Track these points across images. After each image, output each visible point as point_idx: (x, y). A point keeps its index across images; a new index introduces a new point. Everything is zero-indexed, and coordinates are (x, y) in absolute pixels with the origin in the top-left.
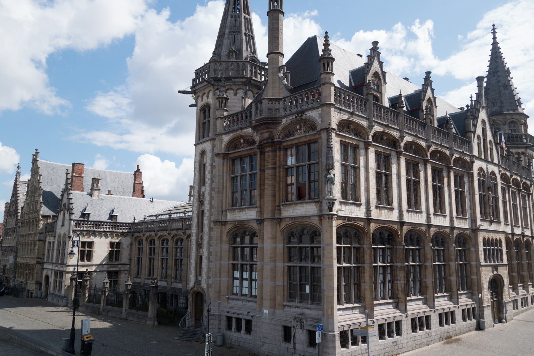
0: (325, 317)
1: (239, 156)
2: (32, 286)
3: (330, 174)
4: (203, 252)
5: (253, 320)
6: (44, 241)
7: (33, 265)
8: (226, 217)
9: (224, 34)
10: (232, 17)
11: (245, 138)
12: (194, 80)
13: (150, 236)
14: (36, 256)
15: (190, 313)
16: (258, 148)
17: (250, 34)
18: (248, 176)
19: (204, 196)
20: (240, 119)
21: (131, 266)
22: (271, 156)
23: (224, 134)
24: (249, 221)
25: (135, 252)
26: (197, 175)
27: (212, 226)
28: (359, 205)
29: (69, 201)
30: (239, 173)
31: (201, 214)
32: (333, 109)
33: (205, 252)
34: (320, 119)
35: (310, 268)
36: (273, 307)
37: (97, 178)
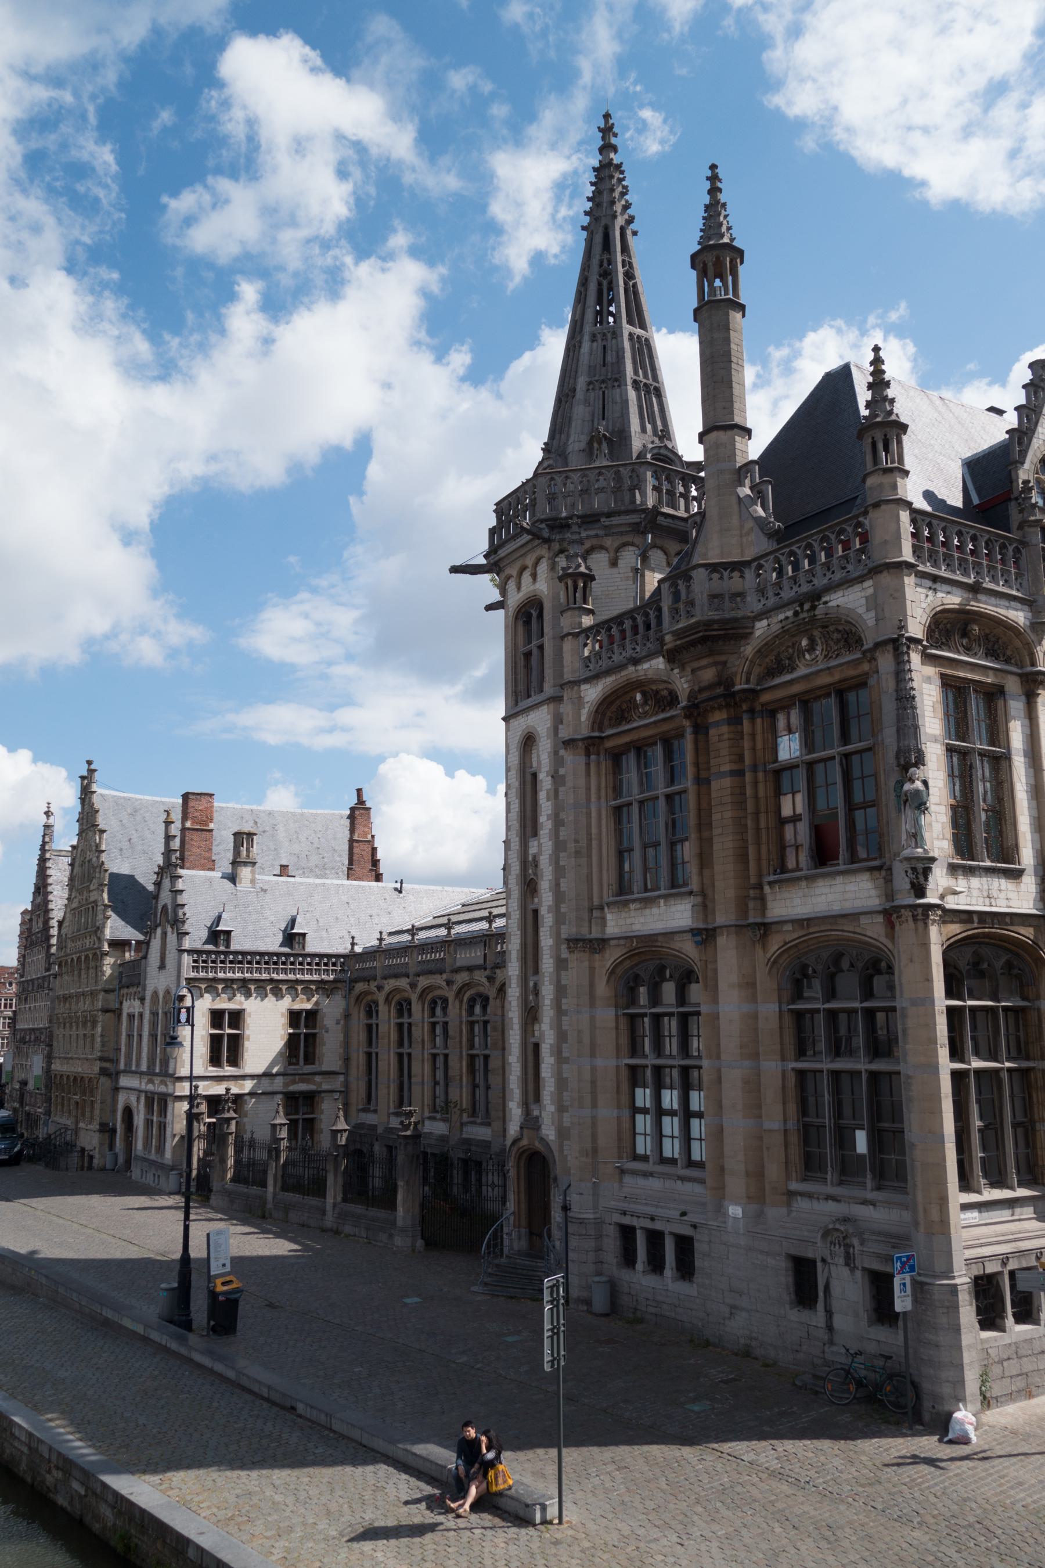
0: (922, 1229)
1: (631, 742)
2: (90, 1139)
3: (912, 781)
4: (542, 1034)
5: (697, 1237)
6: (117, 1012)
7: (90, 1079)
8: (604, 924)
9: (574, 390)
10: (593, 338)
11: (646, 689)
12: (492, 532)
13: (397, 990)
14: (99, 1054)
15: (514, 1213)
16: (687, 717)
17: (650, 381)
18: (662, 802)
19: (536, 866)
20: (628, 634)
21: (352, 1078)
22: (726, 736)
23: (587, 680)
24: (670, 935)
25: (359, 1036)
26: (516, 807)
27: (565, 954)
28: (1016, 875)
29: (174, 899)
30: (633, 791)
31: (531, 920)
32: (909, 581)
33: (546, 1032)
34: (872, 614)
35: (864, 1077)
36: (757, 1197)
37: (246, 830)
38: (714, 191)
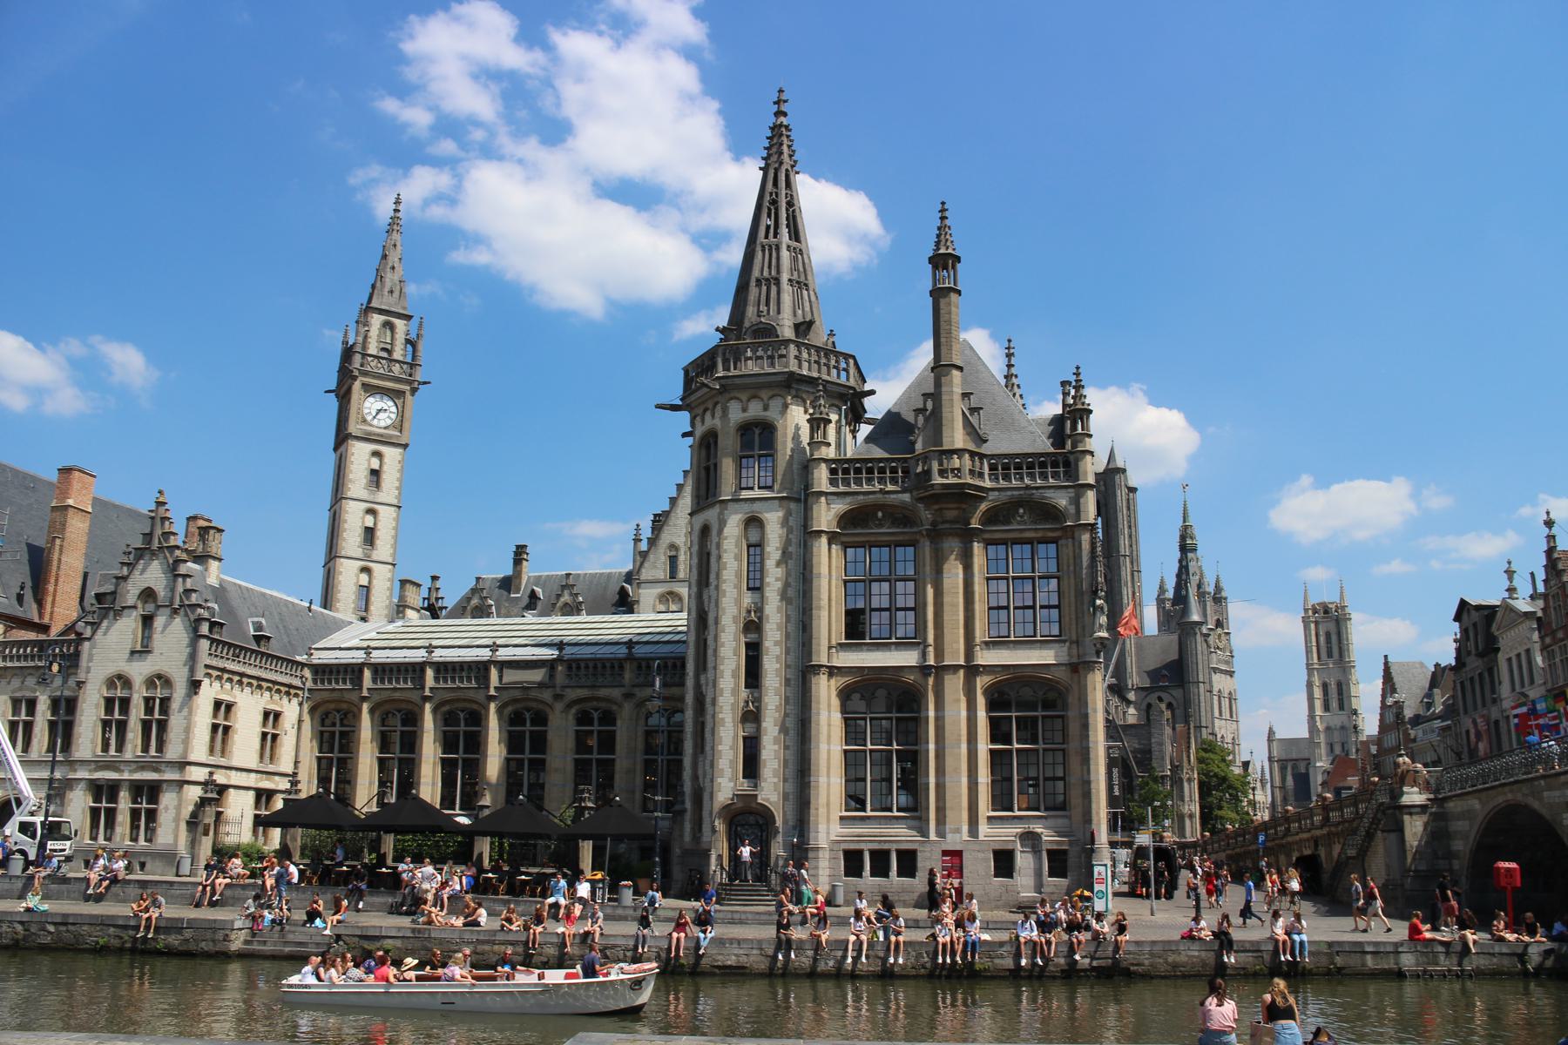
34: (1073, 507)
38: (943, 218)
